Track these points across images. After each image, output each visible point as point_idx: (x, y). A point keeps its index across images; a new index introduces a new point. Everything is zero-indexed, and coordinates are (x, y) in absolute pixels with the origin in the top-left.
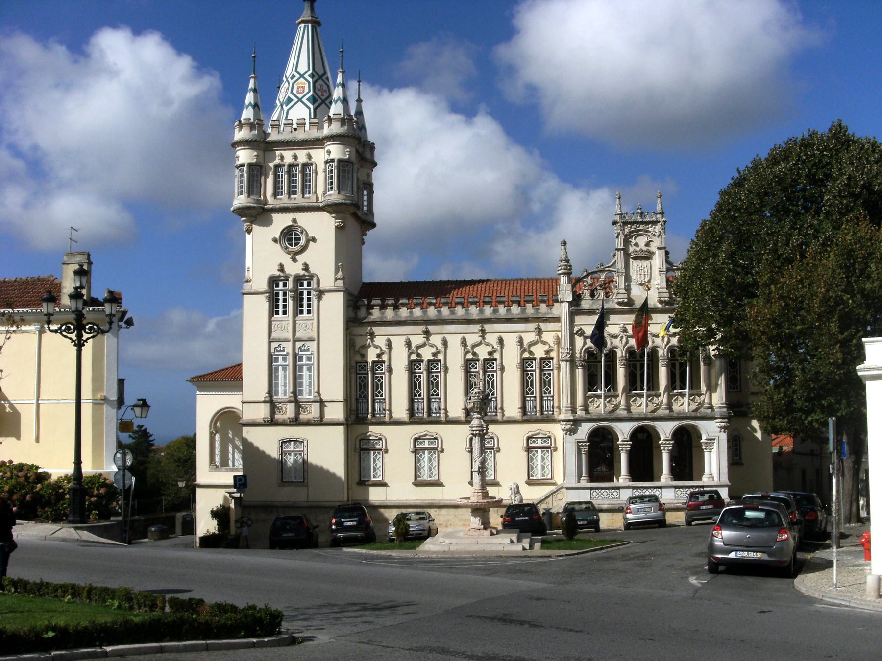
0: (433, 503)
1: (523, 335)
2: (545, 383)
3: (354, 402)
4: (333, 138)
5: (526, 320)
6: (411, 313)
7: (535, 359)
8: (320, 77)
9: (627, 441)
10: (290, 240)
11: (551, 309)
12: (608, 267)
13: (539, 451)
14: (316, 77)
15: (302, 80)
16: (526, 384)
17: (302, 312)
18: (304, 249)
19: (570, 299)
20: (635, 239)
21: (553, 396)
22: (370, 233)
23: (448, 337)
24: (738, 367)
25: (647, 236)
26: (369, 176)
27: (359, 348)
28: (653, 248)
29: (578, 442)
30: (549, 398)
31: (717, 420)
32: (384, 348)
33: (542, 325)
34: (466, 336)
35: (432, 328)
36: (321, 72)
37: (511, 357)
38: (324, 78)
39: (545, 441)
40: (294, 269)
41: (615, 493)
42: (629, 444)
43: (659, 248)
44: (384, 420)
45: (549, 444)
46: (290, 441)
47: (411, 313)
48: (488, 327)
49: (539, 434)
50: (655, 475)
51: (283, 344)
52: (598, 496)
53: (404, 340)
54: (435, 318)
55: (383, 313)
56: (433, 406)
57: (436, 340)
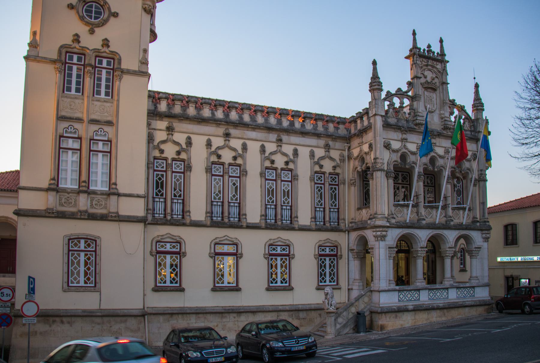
0: (233, 310)
1: (314, 149)
3: (151, 199)
5: (318, 135)
6: (213, 114)
27: (158, 144)
29: (389, 248)
32: (184, 146)
44: (184, 221)
46: (79, 239)
47: (213, 114)
50: (438, 279)
53: (206, 141)
54: (238, 122)
57: (236, 144)
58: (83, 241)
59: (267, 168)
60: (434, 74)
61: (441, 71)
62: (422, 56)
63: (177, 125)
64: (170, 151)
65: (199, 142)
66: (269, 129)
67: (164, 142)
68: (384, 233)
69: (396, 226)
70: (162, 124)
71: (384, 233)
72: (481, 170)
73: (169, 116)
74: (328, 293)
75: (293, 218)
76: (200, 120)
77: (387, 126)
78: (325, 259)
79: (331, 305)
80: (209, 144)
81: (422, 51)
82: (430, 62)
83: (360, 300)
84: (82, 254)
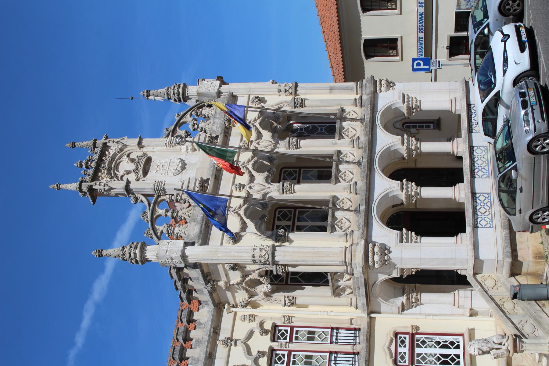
7: (272, 350)
9: (403, 184)
11: (200, 324)
12: (149, 205)
13: (417, 350)
20: (118, 172)
21: (332, 329)
24: (316, 125)
25: (120, 157)
28: (137, 153)
29: (402, 241)
30: (335, 334)
31: (378, 89)
33: (222, 336)
39: (403, 342)
41: (482, 198)
42: (407, 184)
43: (140, 145)
45: (407, 336)
49: (389, 348)
52: (486, 219)
60: (123, 159)
61: (120, 146)
68: (376, 249)
69: (365, 229)
71: (376, 249)
72: (280, 91)
74: (479, 349)
78: (419, 355)
79: (500, 344)
83: (490, 294)
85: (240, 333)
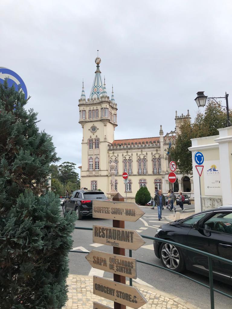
1: (153, 152)
2: (160, 165)
4: (102, 102)
5: (154, 148)
6: (124, 147)
8: (101, 87)
10: (93, 129)
13: (158, 183)
14: (100, 87)
15: (96, 88)
16: (154, 165)
17: (96, 148)
18: (96, 131)
19: (163, 141)
22: (116, 127)
23: (133, 153)
26: (115, 112)
32: (117, 157)
33: (158, 149)
34: (138, 153)
35: (129, 151)
36: (101, 85)
37: (149, 158)
38: (102, 87)
40: (94, 137)
47: (124, 147)
48: (143, 150)
51: (92, 156)
55: (117, 148)
56: (129, 171)
57: (130, 154)
58: (94, 182)
59: (138, 159)
62: (178, 119)
63: (115, 152)
64: (114, 158)
65: (120, 155)
66: (139, 149)
67: (112, 156)
70: (112, 152)
73: (113, 150)
75: (147, 172)
76: (120, 149)
77: (165, 144)
80: (123, 155)
81: (179, 117)
82: (182, 120)
84: (94, 185)
85: (158, 152)
